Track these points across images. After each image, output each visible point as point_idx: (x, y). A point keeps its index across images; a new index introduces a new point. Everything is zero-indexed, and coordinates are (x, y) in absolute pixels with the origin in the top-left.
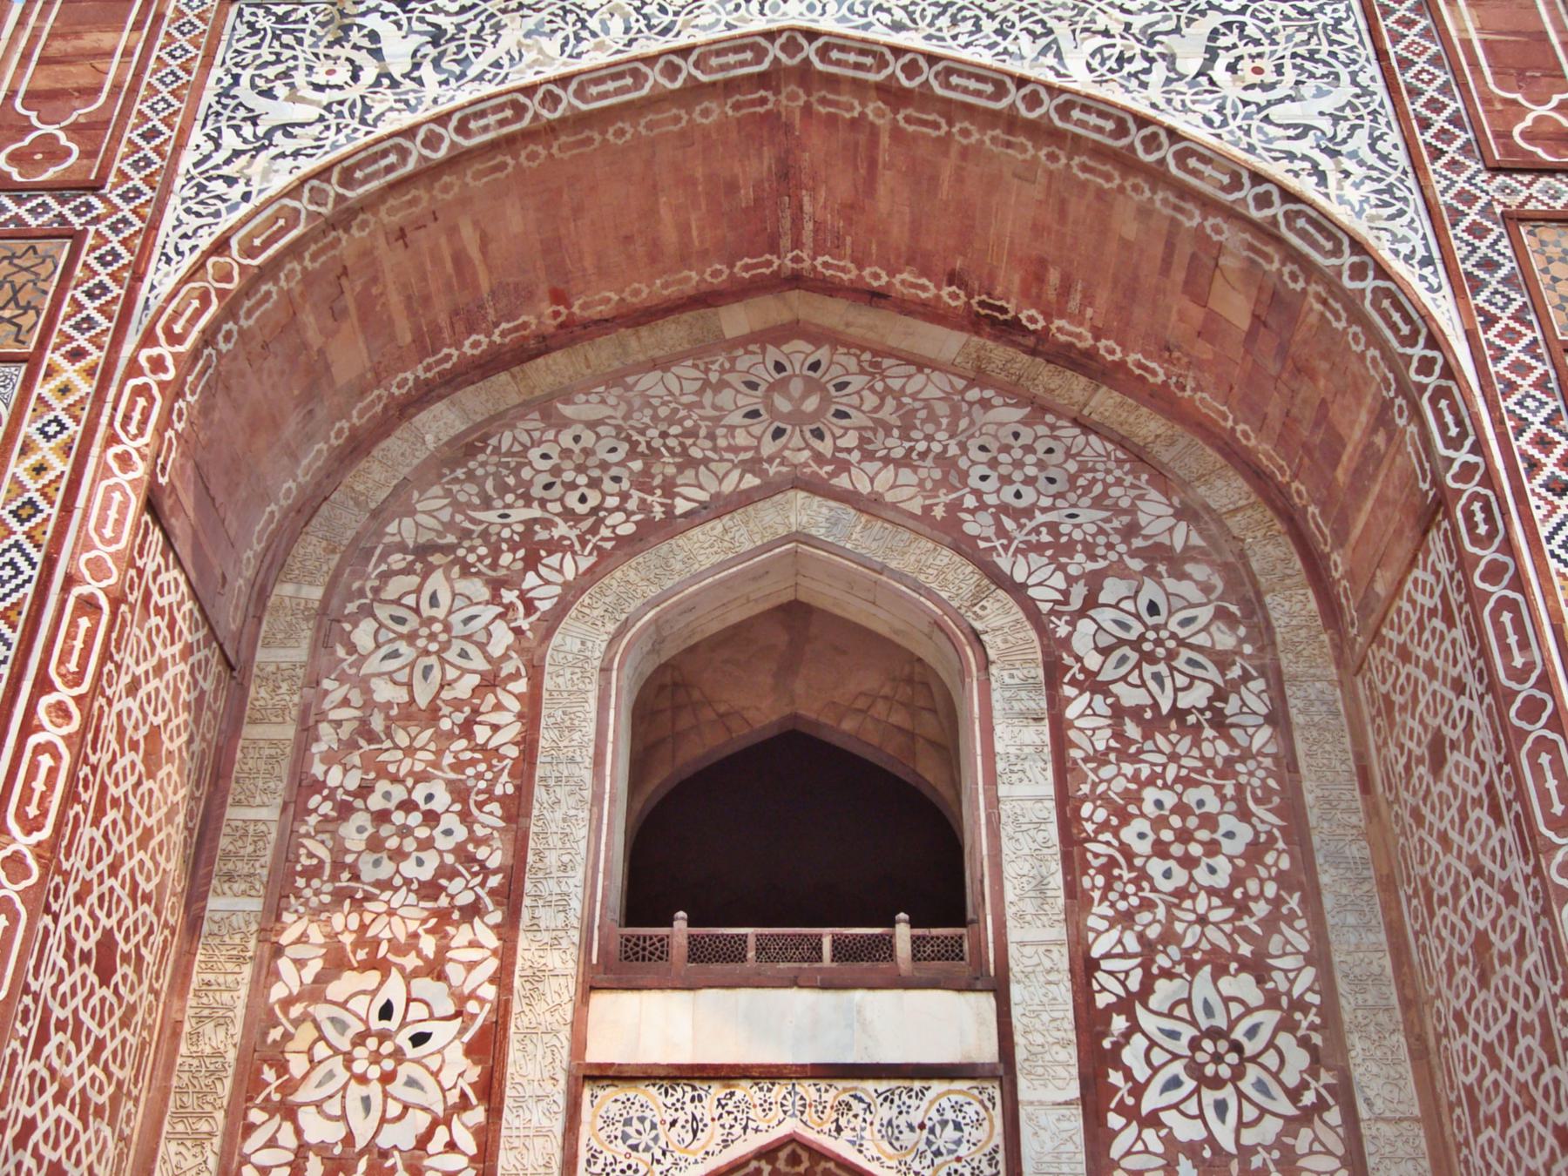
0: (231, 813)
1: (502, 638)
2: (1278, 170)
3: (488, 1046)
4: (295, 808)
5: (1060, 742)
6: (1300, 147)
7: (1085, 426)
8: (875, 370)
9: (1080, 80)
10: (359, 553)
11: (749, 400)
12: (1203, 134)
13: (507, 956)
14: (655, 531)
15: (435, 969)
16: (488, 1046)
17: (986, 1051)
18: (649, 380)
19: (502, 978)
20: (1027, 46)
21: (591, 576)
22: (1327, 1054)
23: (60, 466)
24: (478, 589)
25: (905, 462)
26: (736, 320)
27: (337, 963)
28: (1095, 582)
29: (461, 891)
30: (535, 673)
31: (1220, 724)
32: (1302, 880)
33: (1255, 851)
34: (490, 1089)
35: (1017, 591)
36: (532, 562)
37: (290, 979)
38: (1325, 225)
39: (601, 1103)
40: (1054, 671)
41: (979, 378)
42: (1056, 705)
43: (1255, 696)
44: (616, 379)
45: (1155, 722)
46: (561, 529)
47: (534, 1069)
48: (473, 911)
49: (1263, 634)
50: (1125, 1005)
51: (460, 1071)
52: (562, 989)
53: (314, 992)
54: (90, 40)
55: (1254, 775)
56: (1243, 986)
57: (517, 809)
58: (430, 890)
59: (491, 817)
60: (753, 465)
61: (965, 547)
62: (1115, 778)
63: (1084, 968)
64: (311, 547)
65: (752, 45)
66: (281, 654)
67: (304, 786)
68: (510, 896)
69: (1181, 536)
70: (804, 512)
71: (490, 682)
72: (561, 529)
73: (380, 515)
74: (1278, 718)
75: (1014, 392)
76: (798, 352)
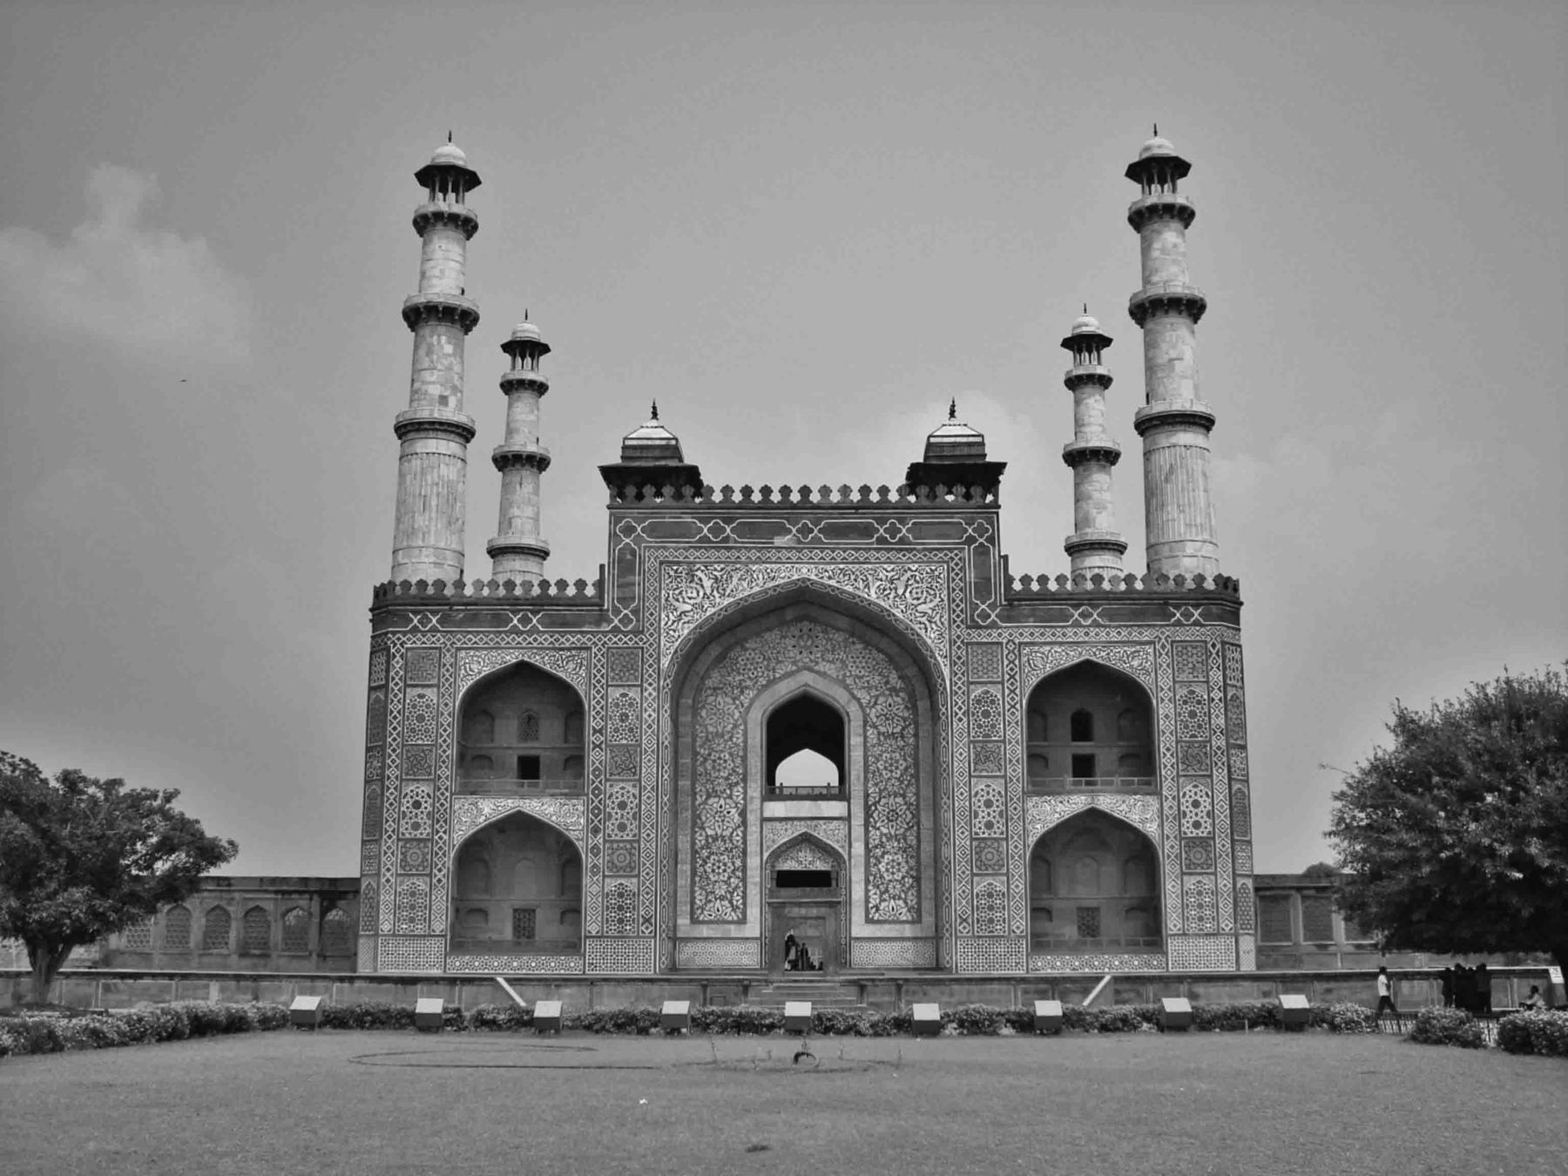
0: (682, 761)
1: (737, 715)
2: (916, 627)
3: (743, 814)
4: (694, 760)
5: (865, 742)
6: (924, 620)
7: (880, 651)
8: (825, 632)
9: (873, 596)
10: (699, 690)
11: (793, 642)
12: (900, 615)
13: (745, 793)
14: (771, 682)
15: (730, 797)
16: (743, 814)
17: (845, 814)
18: (767, 635)
19: (745, 799)
20: (861, 585)
21: (757, 696)
22: (916, 816)
23: (654, 715)
24: (729, 700)
25: (832, 662)
26: (790, 614)
27: (709, 796)
28: (877, 697)
29: (734, 779)
30: (745, 723)
31: (903, 737)
32: (916, 776)
33: (906, 769)
34: (744, 823)
35: (858, 700)
36: (742, 692)
37: (699, 800)
38: (925, 643)
39: (767, 826)
40: (865, 723)
41: (852, 635)
42: (865, 731)
43: (911, 730)
44: (758, 634)
45: (888, 736)
46: (749, 683)
47: (752, 818)
48: (737, 784)
49: (916, 713)
50: (875, 804)
51: (737, 819)
52: (757, 802)
53: (705, 802)
54: (629, 579)
55: (909, 750)
56: (899, 800)
57: (744, 759)
58: (727, 779)
59: (739, 760)
60: (794, 663)
61: (846, 687)
62: (877, 751)
63: (867, 796)
64: (686, 690)
65: (795, 582)
66: (686, 719)
67: (696, 754)
68: (745, 780)
69: (899, 684)
70: (807, 678)
71: (735, 726)
72: (749, 683)
73: (702, 679)
74: (916, 735)
75: (861, 639)
76: (806, 625)
